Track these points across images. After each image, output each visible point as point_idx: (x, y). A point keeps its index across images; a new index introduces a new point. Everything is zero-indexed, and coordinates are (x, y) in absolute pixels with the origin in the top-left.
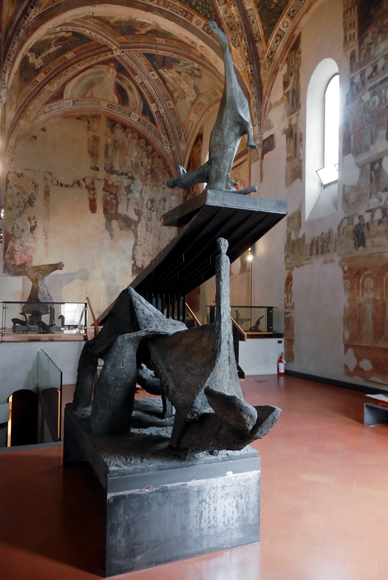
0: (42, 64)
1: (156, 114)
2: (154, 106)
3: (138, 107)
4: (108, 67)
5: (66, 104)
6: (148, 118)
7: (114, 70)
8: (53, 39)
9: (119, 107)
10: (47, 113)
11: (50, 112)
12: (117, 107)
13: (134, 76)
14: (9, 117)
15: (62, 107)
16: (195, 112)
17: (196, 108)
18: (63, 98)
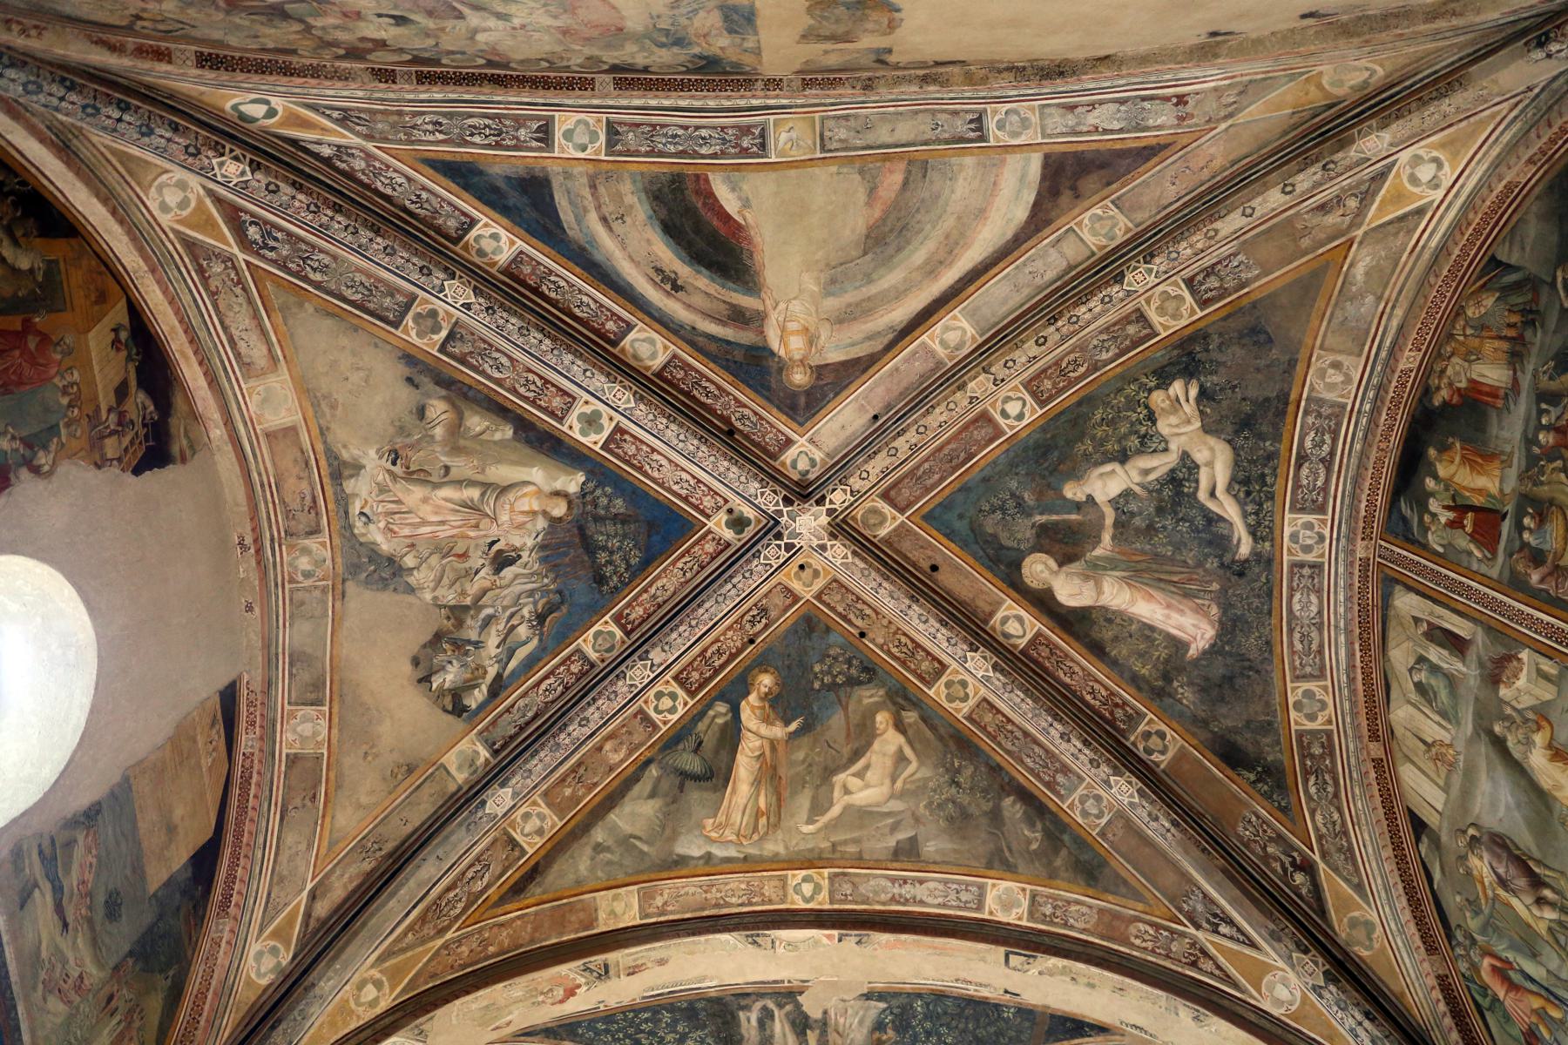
0: (1158, 399)
1: (464, 214)
2: (498, 250)
3: (589, 201)
4: (816, 361)
5: (1025, 124)
6: (497, 170)
7: (782, 353)
8: (1111, 564)
9: (697, 155)
10: (1167, 99)
11: (1144, 99)
12: (704, 151)
13: (675, 356)
14: (1448, 174)
15: (1053, 110)
16: (291, 431)
17: (307, 463)
18: (1047, 157)
